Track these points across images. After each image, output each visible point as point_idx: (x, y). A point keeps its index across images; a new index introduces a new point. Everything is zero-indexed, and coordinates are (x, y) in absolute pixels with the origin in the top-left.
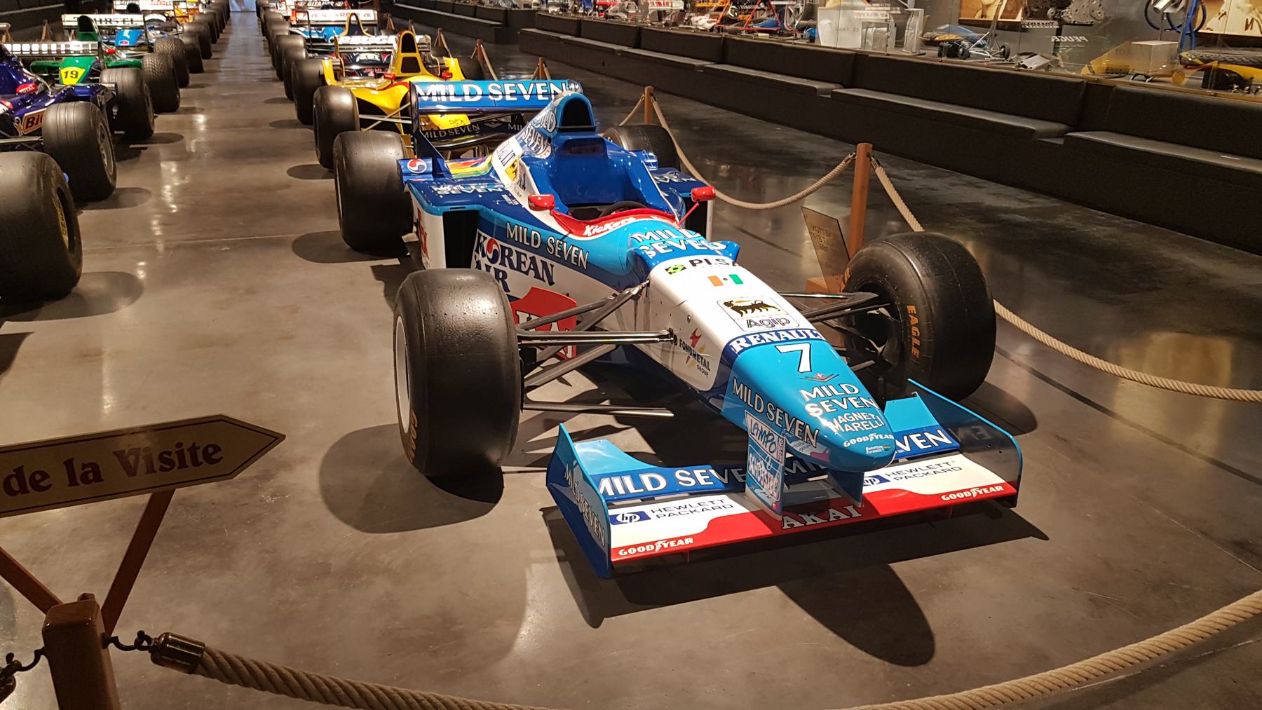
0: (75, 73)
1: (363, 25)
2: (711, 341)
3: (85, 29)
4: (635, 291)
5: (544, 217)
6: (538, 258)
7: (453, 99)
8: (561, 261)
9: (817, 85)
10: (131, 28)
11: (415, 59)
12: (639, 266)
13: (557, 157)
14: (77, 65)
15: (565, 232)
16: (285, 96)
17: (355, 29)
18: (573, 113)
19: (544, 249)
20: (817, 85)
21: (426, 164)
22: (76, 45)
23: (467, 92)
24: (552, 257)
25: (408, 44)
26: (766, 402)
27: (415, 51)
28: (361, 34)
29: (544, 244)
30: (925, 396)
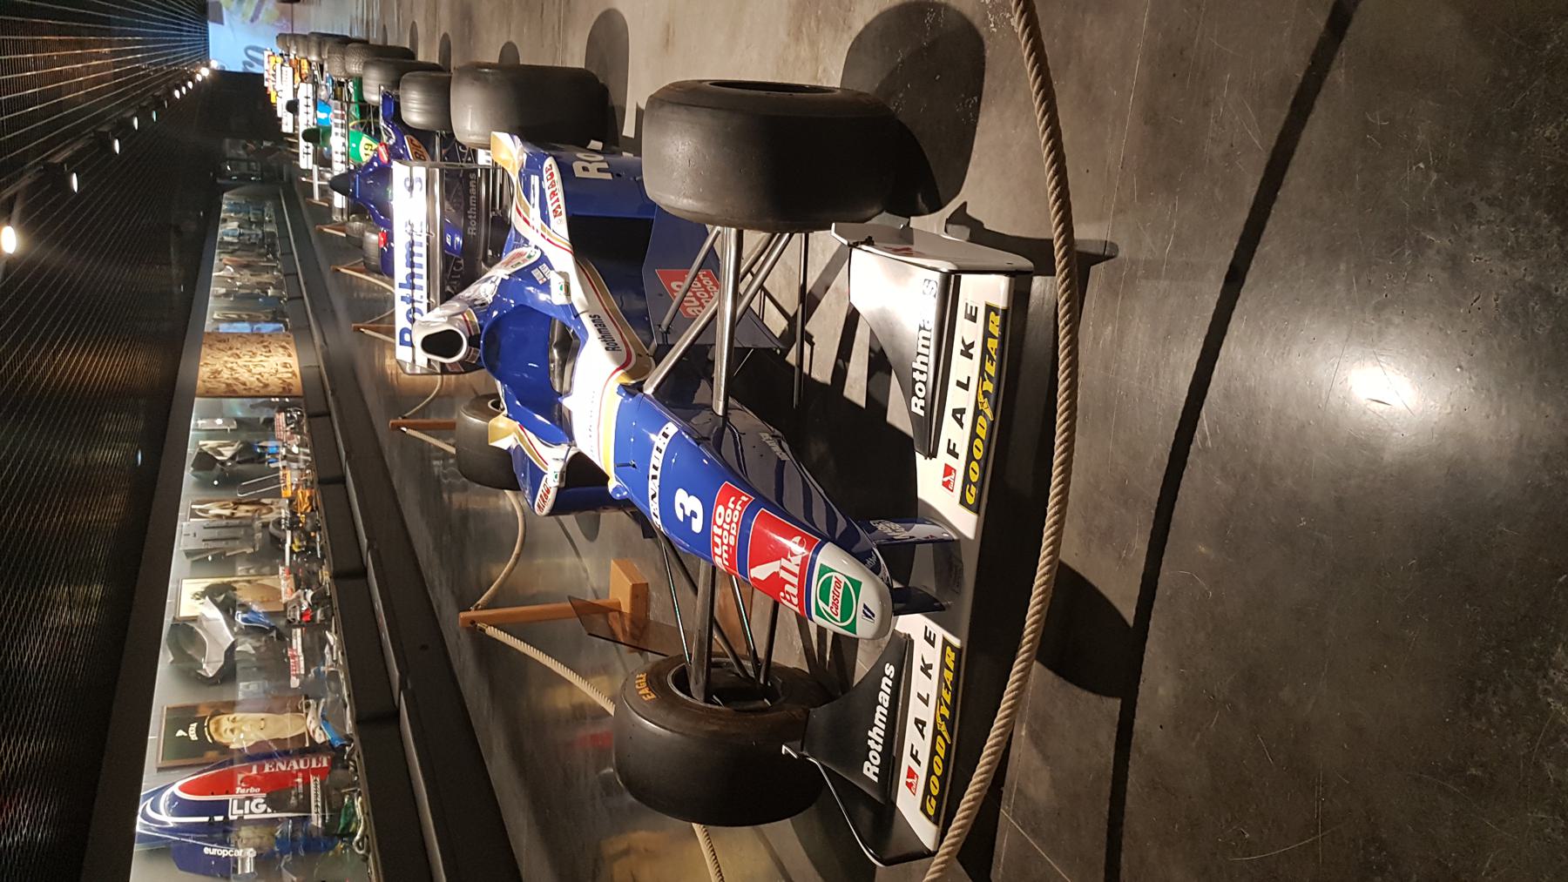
0: (367, 147)
3: (317, 136)
10: (316, 108)
14: (358, 145)
22: (337, 143)
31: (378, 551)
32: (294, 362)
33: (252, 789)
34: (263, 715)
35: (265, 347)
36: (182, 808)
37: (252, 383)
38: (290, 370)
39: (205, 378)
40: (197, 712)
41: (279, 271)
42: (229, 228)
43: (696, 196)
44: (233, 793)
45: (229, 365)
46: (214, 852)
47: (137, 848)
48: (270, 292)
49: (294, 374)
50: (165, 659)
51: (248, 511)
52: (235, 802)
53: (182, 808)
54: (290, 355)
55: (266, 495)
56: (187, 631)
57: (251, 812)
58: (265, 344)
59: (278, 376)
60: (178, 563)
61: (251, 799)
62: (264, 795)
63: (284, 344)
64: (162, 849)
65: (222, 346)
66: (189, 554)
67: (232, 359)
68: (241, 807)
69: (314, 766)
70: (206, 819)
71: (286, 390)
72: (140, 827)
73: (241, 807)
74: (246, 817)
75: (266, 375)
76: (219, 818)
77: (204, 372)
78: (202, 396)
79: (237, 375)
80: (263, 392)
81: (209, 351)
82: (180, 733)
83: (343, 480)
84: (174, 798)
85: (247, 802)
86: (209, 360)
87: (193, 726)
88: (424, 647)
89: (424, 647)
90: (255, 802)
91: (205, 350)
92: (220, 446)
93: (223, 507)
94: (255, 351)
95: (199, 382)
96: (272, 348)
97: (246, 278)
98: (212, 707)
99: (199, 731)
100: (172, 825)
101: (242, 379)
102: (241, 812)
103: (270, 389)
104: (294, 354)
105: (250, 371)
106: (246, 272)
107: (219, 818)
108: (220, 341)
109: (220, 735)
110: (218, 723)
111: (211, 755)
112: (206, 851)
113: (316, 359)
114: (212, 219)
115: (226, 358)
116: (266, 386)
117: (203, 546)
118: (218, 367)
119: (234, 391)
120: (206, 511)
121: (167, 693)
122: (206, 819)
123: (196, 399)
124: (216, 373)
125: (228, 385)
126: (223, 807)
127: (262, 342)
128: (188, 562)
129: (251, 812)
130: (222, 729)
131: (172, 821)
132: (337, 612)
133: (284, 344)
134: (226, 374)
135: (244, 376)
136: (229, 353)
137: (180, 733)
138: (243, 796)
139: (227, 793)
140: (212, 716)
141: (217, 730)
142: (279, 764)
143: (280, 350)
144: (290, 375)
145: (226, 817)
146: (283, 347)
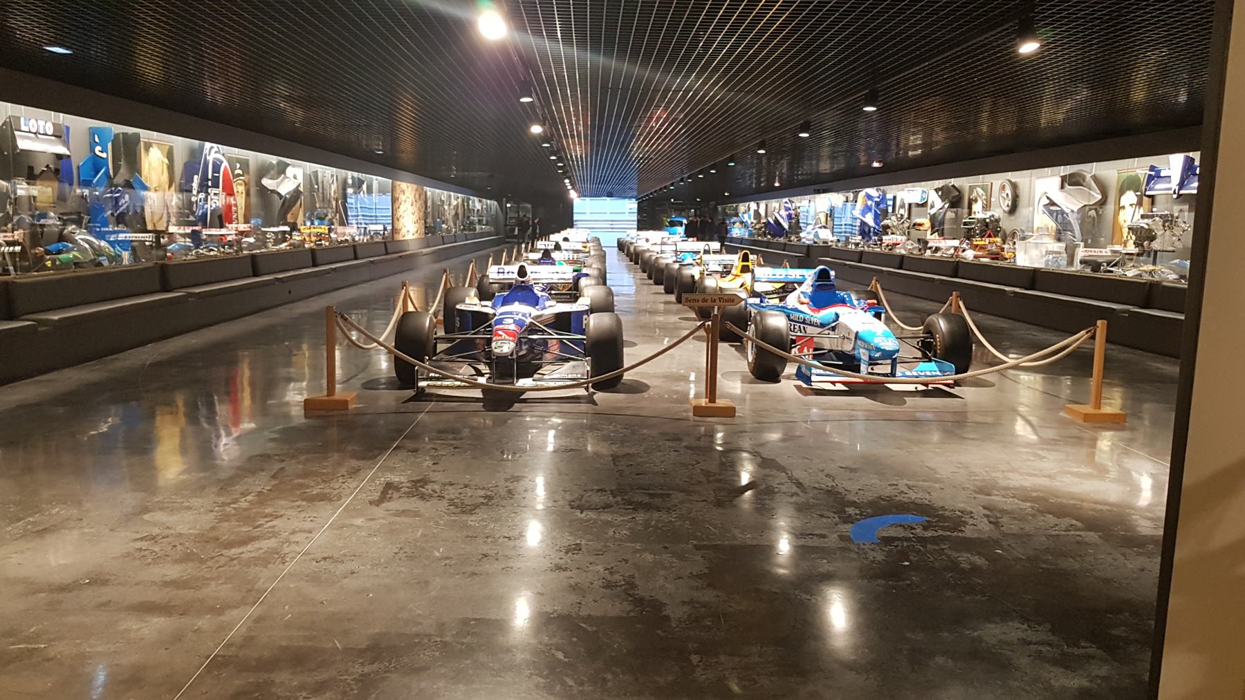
2: (852, 331)
4: (833, 324)
5: (804, 308)
6: (802, 326)
8: (810, 325)
9: (1007, 289)
11: (748, 266)
12: (837, 316)
13: (814, 292)
15: (812, 313)
16: (663, 291)
17: (706, 252)
18: (823, 275)
19: (804, 322)
20: (1007, 289)
21: (757, 301)
24: (808, 324)
25: (745, 258)
26: (870, 348)
27: (748, 261)
29: (804, 320)
30: (936, 361)
31: (274, 284)
41: (456, 232)
42: (477, 204)
43: (594, 328)
44: (223, 191)
47: (197, 142)
48: (444, 226)
49: (404, 236)
50: (274, 159)
55: (341, 216)
56: (281, 170)
57: (211, 199)
65: (417, 196)
66: (316, 173)
71: (395, 231)
72: (208, 145)
73: (215, 194)
77: (404, 185)
78: (393, 183)
80: (395, 217)
82: (238, 165)
83: (356, 258)
84: (222, 162)
86: (410, 189)
87: (240, 172)
88: (290, 292)
89: (290, 292)
91: (415, 186)
93: (335, 192)
95: (399, 183)
97: (449, 213)
101: (402, 207)
106: (453, 213)
110: (241, 184)
112: (196, 177)
113: (413, 249)
114: (482, 194)
116: (398, 220)
117: (320, 180)
118: (407, 194)
123: (390, 181)
124: (403, 192)
125: (398, 199)
129: (211, 199)
132: (295, 250)
134: (402, 197)
135: (403, 208)
137: (238, 165)
139: (223, 188)
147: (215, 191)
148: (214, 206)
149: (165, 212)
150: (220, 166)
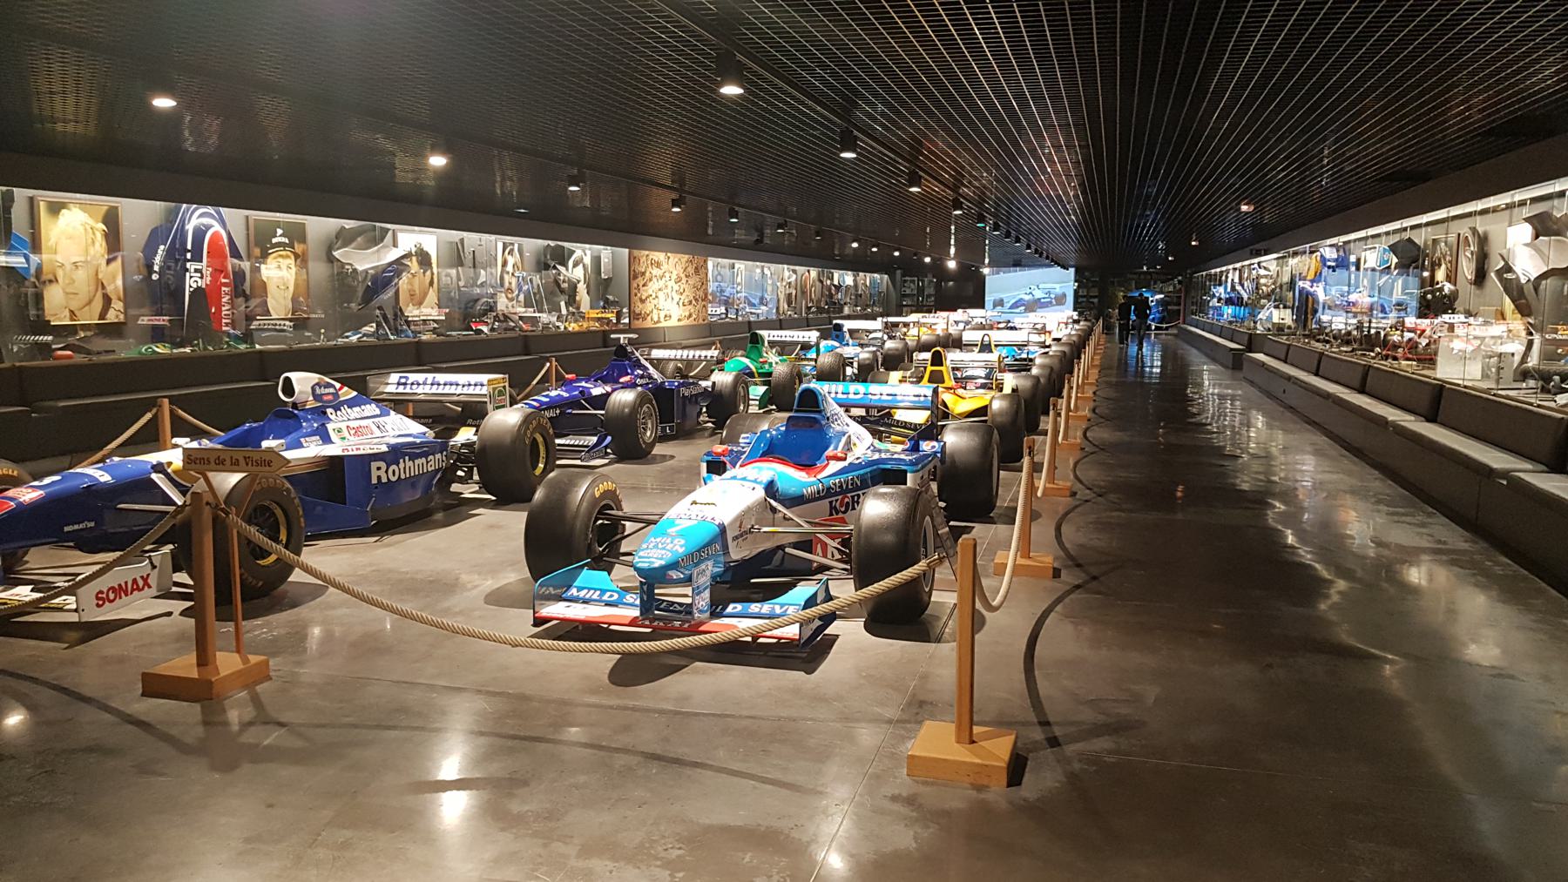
1: (996, 346)
7: (840, 396)
11: (941, 371)
23: (851, 391)
28: (991, 351)
32: (673, 322)
33: (209, 278)
34: (291, 289)
35: (690, 302)
36: (199, 234)
37: (646, 291)
38: (662, 319)
39: (651, 257)
40: (299, 242)
45: (667, 275)
46: (160, 252)
49: (659, 322)
50: (349, 224)
51: (510, 283)
52: (200, 267)
53: (199, 234)
54: (679, 320)
57: (191, 277)
58: (694, 302)
59: (655, 311)
60: (454, 235)
61: (202, 278)
62: (204, 286)
63: (694, 316)
64: (171, 216)
65: (691, 270)
66: (462, 240)
67: (674, 277)
68: (196, 271)
69: (224, 321)
70: (189, 247)
73: (196, 271)
74: (188, 274)
75: (656, 302)
76: (189, 256)
77: (659, 256)
79: (654, 279)
80: (635, 299)
81: (684, 260)
82: (280, 232)
84: (208, 227)
85: (199, 275)
90: (199, 280)
92: (584, 266)
94: (685, 294)
95: (647, 252)
96: (690, 307)
98: (303, 254)
99: (279, 244)
100: (187, 227)
101: (650, 284)
102: (192, 270)
103: (639, 304)
104: (681, 324)
105: (660, 290)
107: (189, 256)
108: (696, 268)
109: (275, 258)
110: (288, 257)
111: (257, 251)
112: (162, 247)
115: (675, 273)
118: (665, 267)
119: (635, 277)
120: (511, 253)
121: (319, 227)
122: (189, 247)
123: (627, 250)
125: (643, 274)
126: (197, 258)
127: (696, 300)
128: (457, 240)
129: (191, 277)
130: (280, 260)
131: (190, 228)
132: (381, 342)
133: (694, 316)
135: (653, 287)
136: (683, 276)
137: (280, 232)
138: (204, 272)
140: (297, 256)
141: (281, 256)
142: (228, 297)
143: (687, 314)
144: (656, 319)
145: (189, 261)
146: (690, 316)
147: (198, 266)
148: (195, 285)
149: (99, 294)
150: (205, 232)
